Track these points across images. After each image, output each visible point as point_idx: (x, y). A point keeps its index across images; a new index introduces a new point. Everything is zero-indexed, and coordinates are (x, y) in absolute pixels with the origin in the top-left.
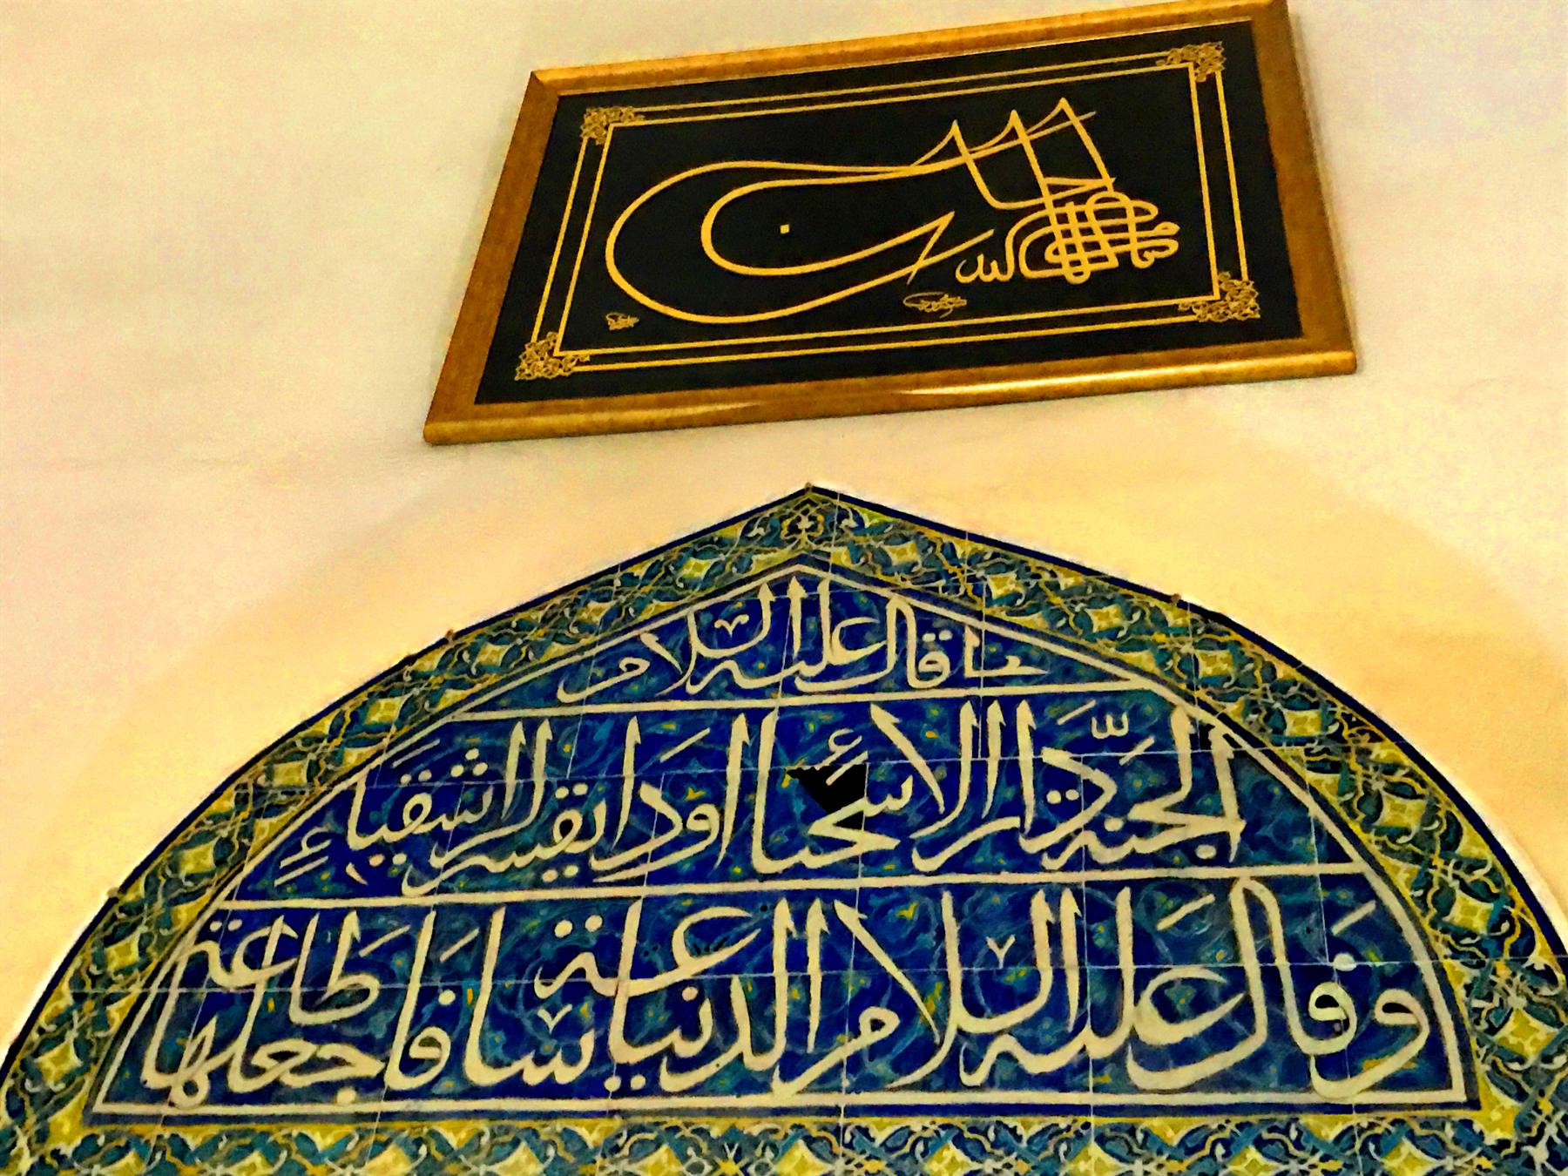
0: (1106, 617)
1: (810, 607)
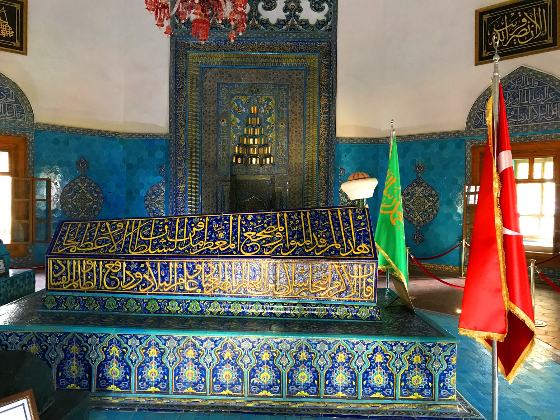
0: (6, 81)
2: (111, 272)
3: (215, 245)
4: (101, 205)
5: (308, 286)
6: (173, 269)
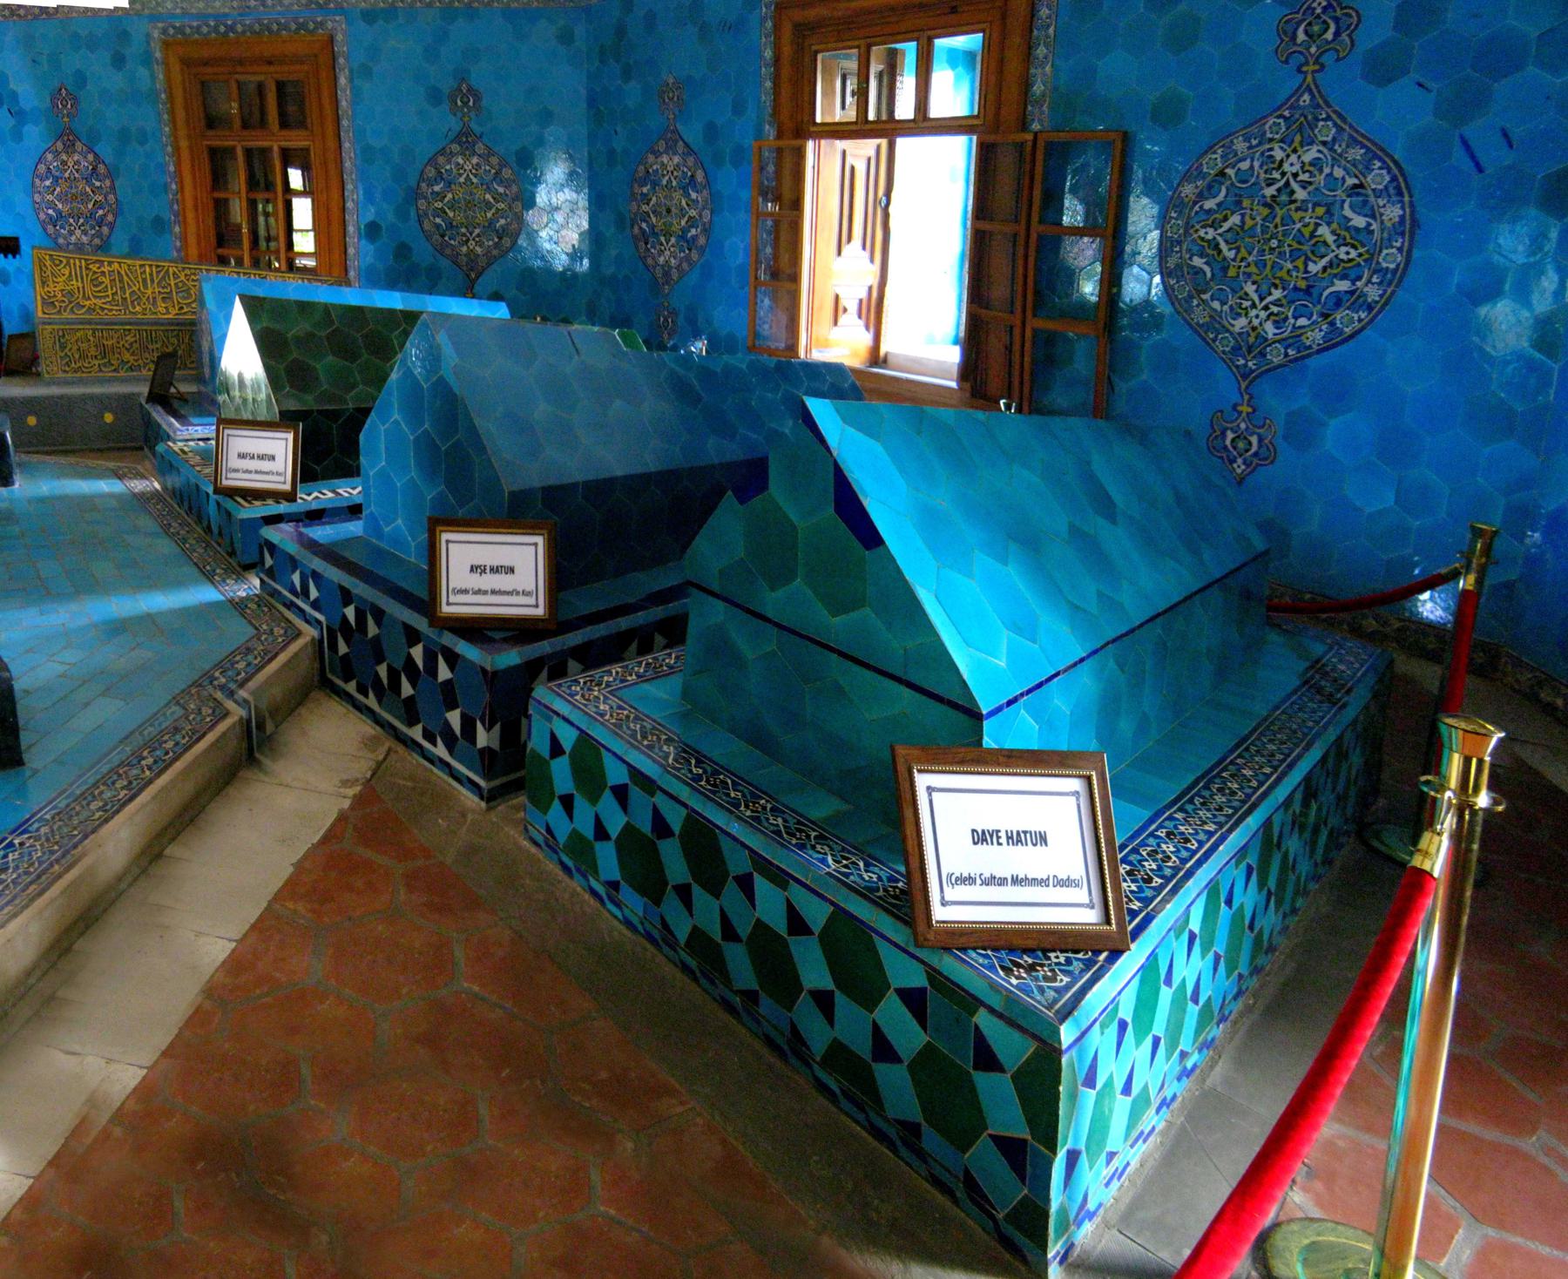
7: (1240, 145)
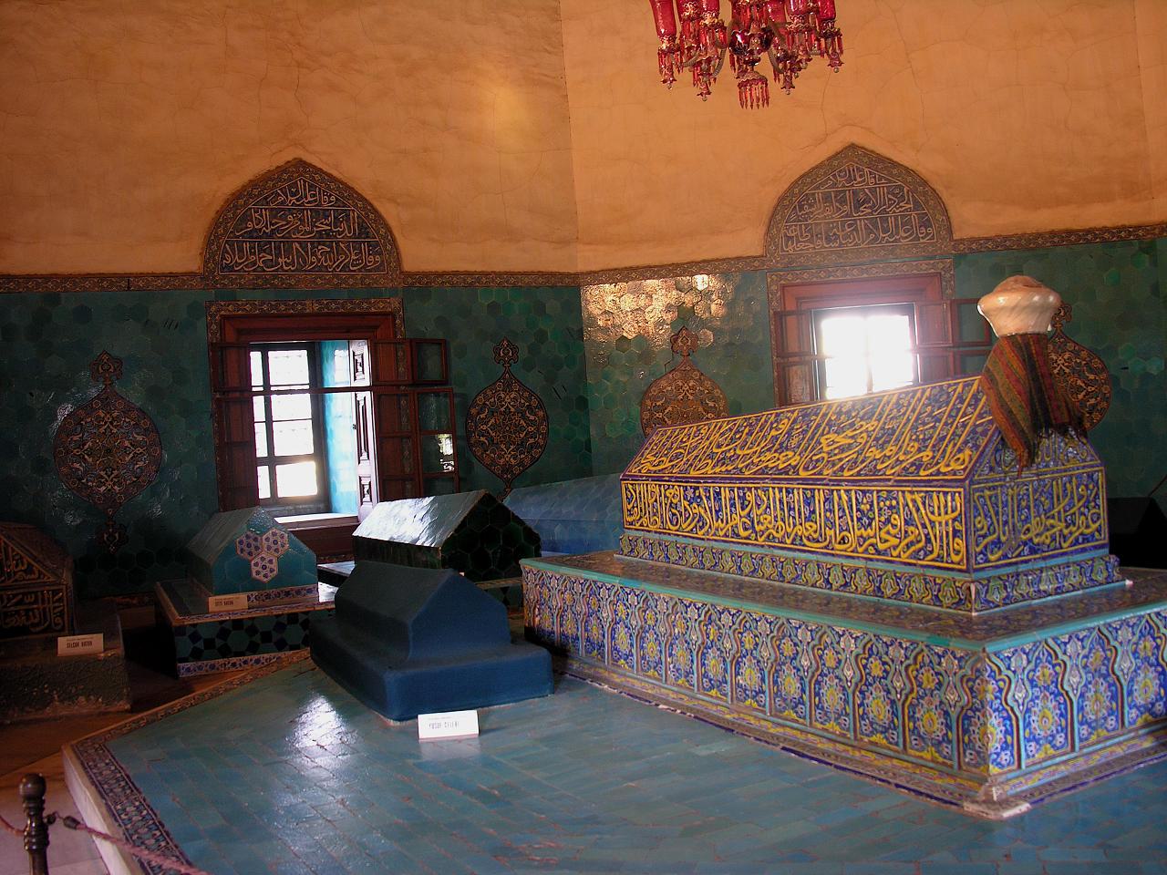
1: (853, 170)
2: (672, 503)
3: (778, 459)
4: (1107, 400)
5: (875, 536)
6: (725, 498)
7: (489, 393)
